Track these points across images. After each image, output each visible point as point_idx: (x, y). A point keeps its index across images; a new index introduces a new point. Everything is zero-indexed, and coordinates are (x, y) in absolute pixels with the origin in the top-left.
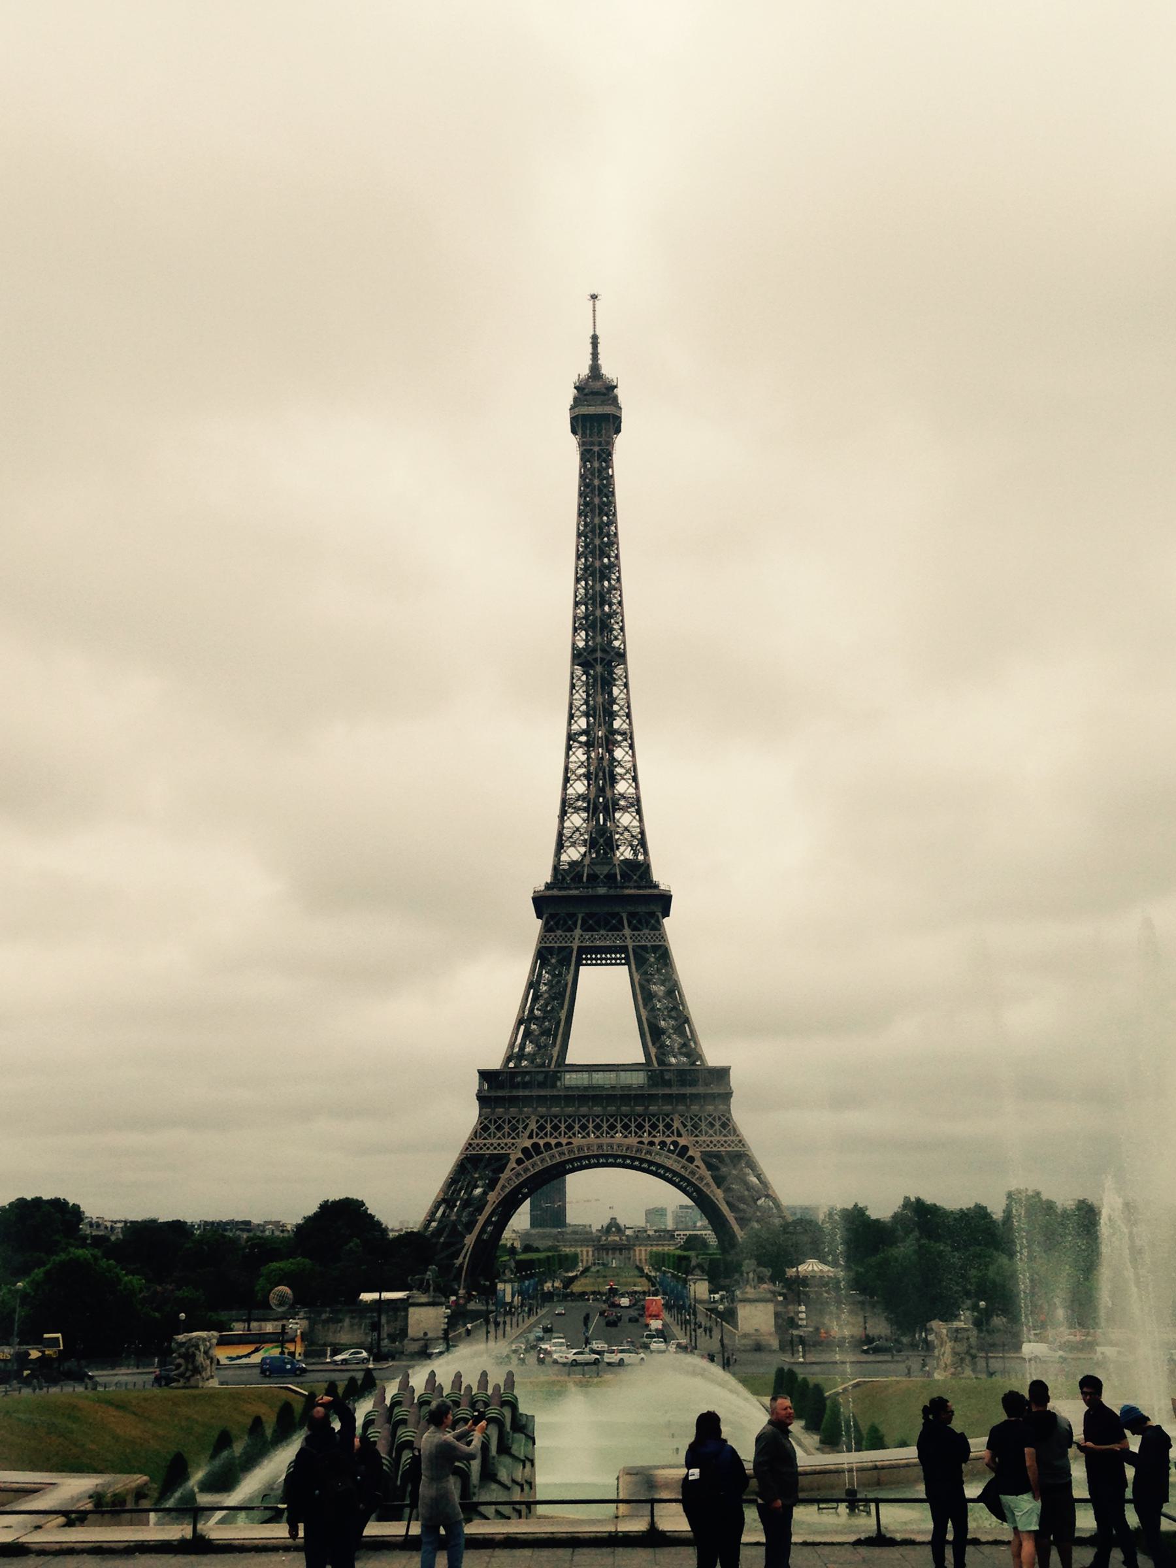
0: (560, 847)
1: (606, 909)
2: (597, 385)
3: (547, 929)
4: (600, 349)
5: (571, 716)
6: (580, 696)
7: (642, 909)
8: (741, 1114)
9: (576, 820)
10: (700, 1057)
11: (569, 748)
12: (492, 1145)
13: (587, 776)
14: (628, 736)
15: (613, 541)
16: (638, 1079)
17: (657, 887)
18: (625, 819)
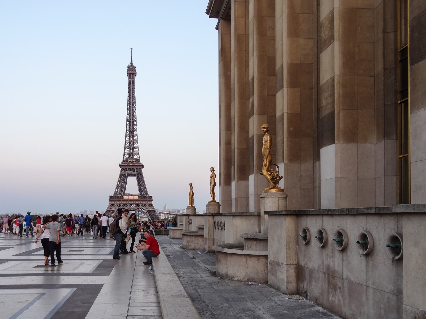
0: (124, 155)
1: (132, 167)
2: (132, 67)
3: (122, 171)
4: (133, 59)
5: (126, 131)
6: (128, 128)
7: (138, 168)
8: (154, 203)
9: (127, 151)
10: (147, 194)
11: (126, 137)
12: (112, 208)
13: (129, 143)
14: (137, 136)
15: (134, 99)
16: (137, 198)
17: (140, 163)
18: (136, 151)
